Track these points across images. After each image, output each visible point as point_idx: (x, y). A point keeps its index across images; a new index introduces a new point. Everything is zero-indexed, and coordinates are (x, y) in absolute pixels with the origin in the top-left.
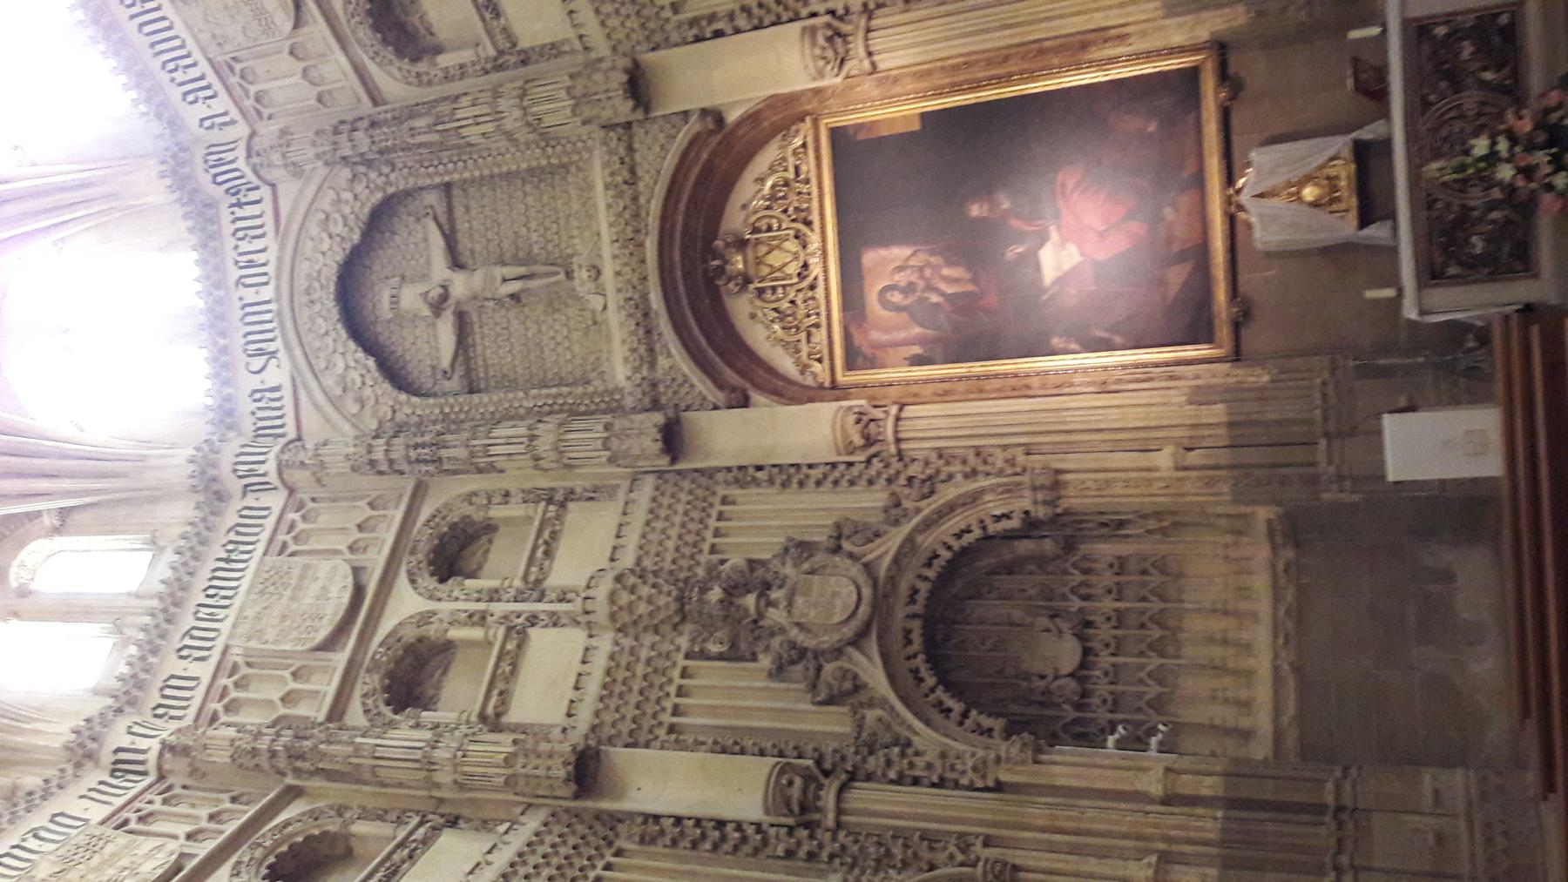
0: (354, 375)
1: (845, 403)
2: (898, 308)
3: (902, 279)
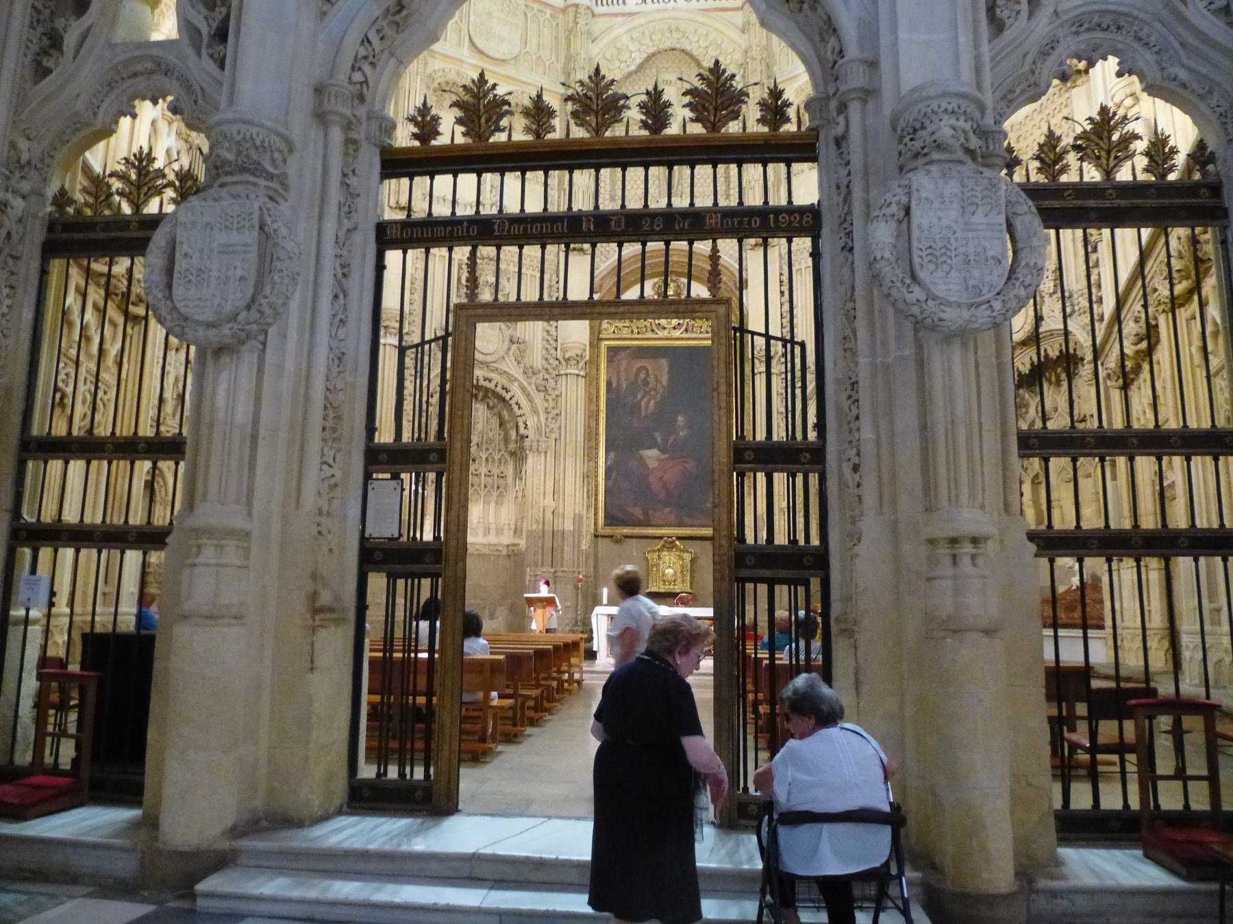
0: (625, 56)
1: (588, 348)
2: (637, 375)
3: (651, 379)
